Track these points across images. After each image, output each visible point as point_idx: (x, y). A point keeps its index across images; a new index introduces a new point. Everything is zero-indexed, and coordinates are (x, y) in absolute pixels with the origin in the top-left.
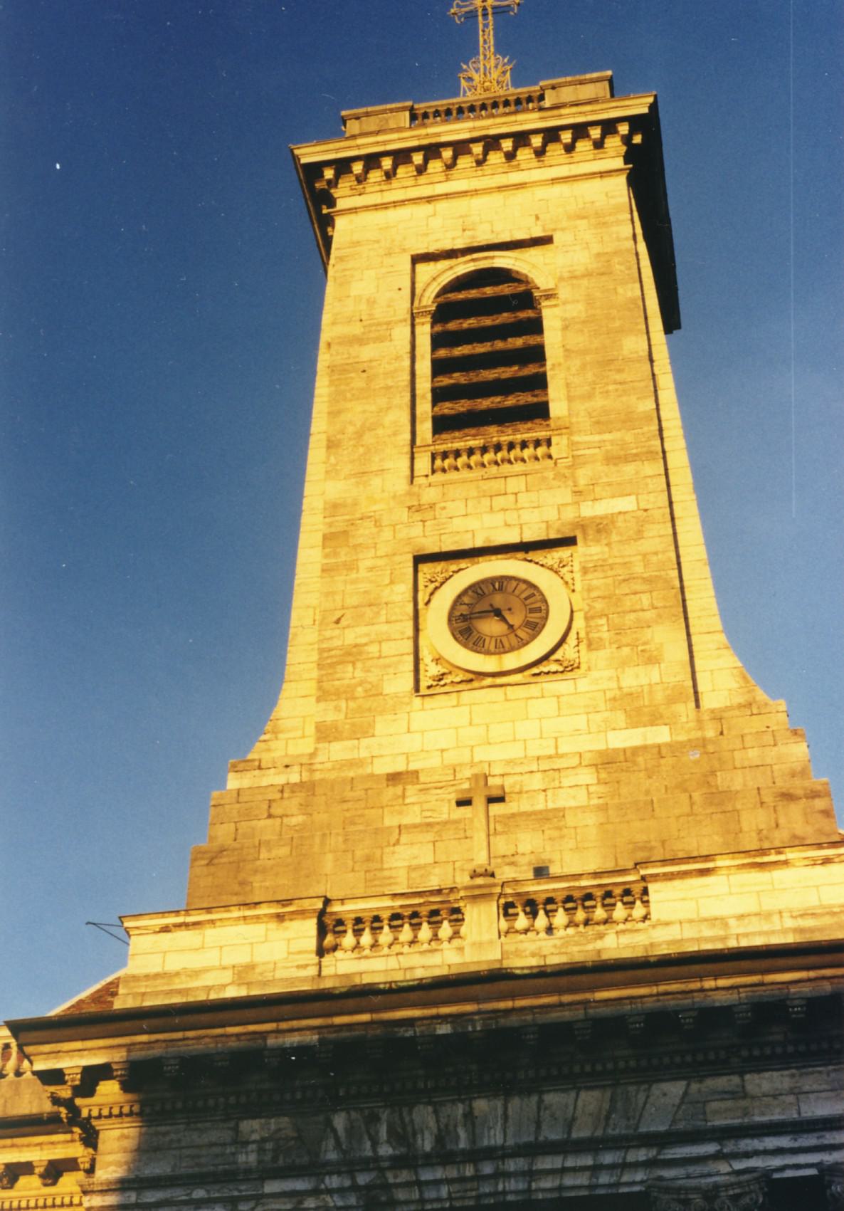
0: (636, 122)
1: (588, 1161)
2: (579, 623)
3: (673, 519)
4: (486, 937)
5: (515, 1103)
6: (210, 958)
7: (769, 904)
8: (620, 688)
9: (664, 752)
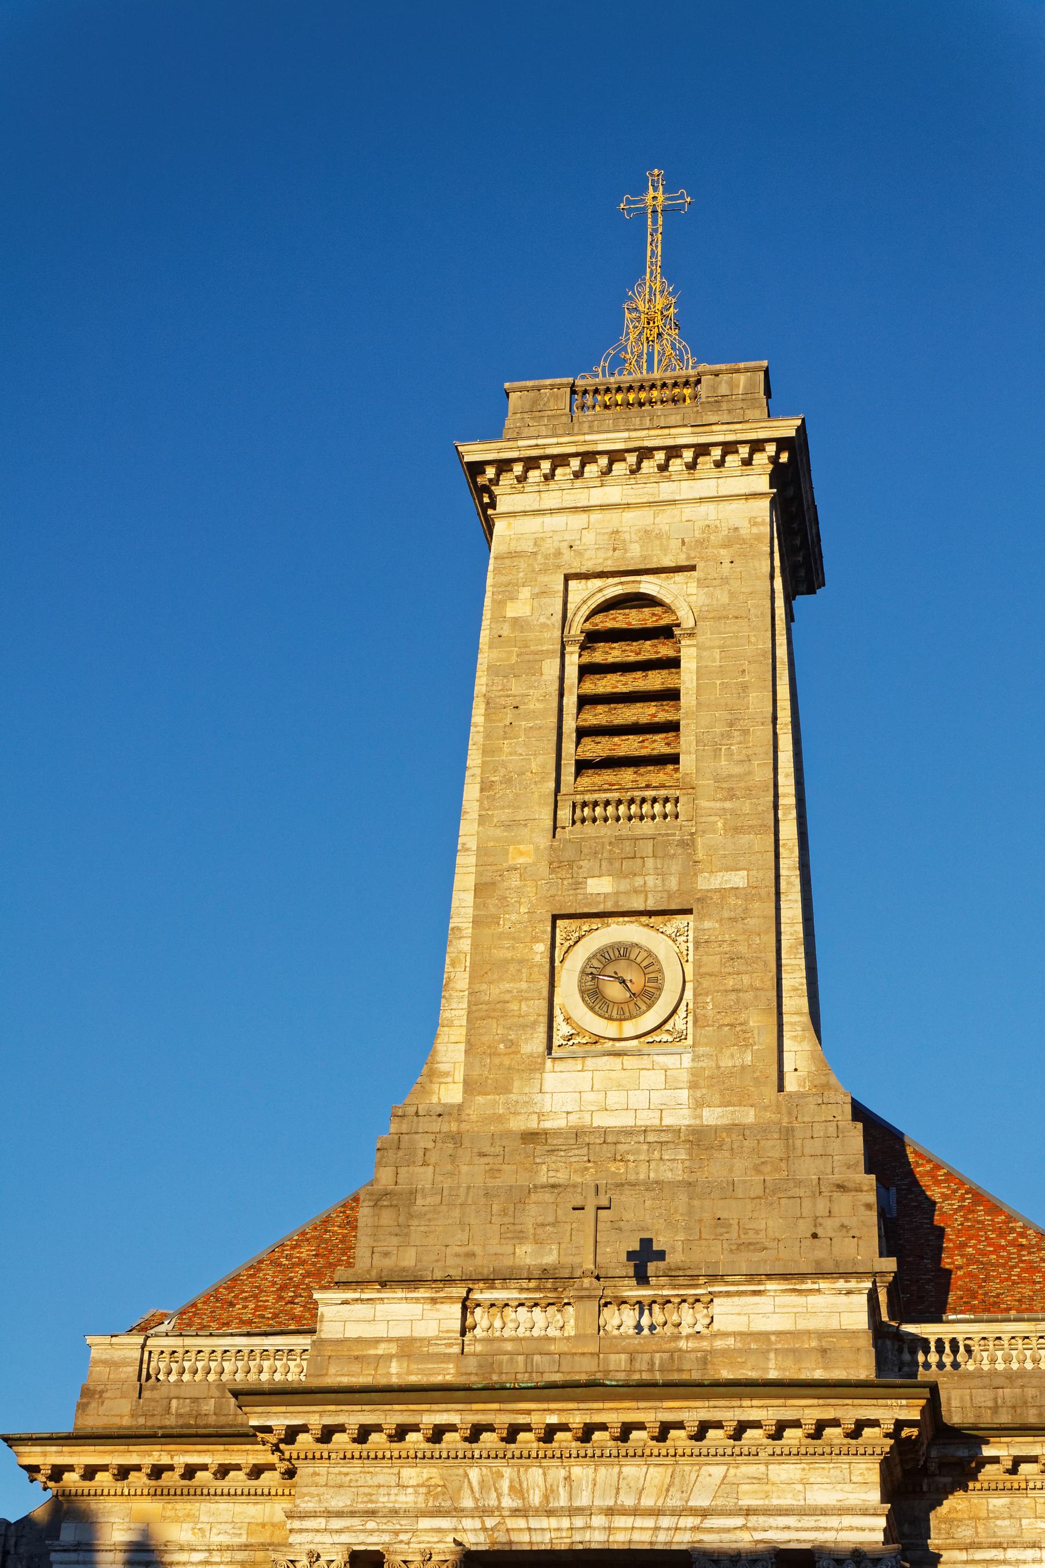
0: (782, 444)
1: (649, 1522)
2: (689, 995)
3: (778, 893)
4: (589, 1331)
5: (602, 1470)
6: (378, 1331)
7: (803, 1325)
8: (718, 1067)
9: (747, 1132)
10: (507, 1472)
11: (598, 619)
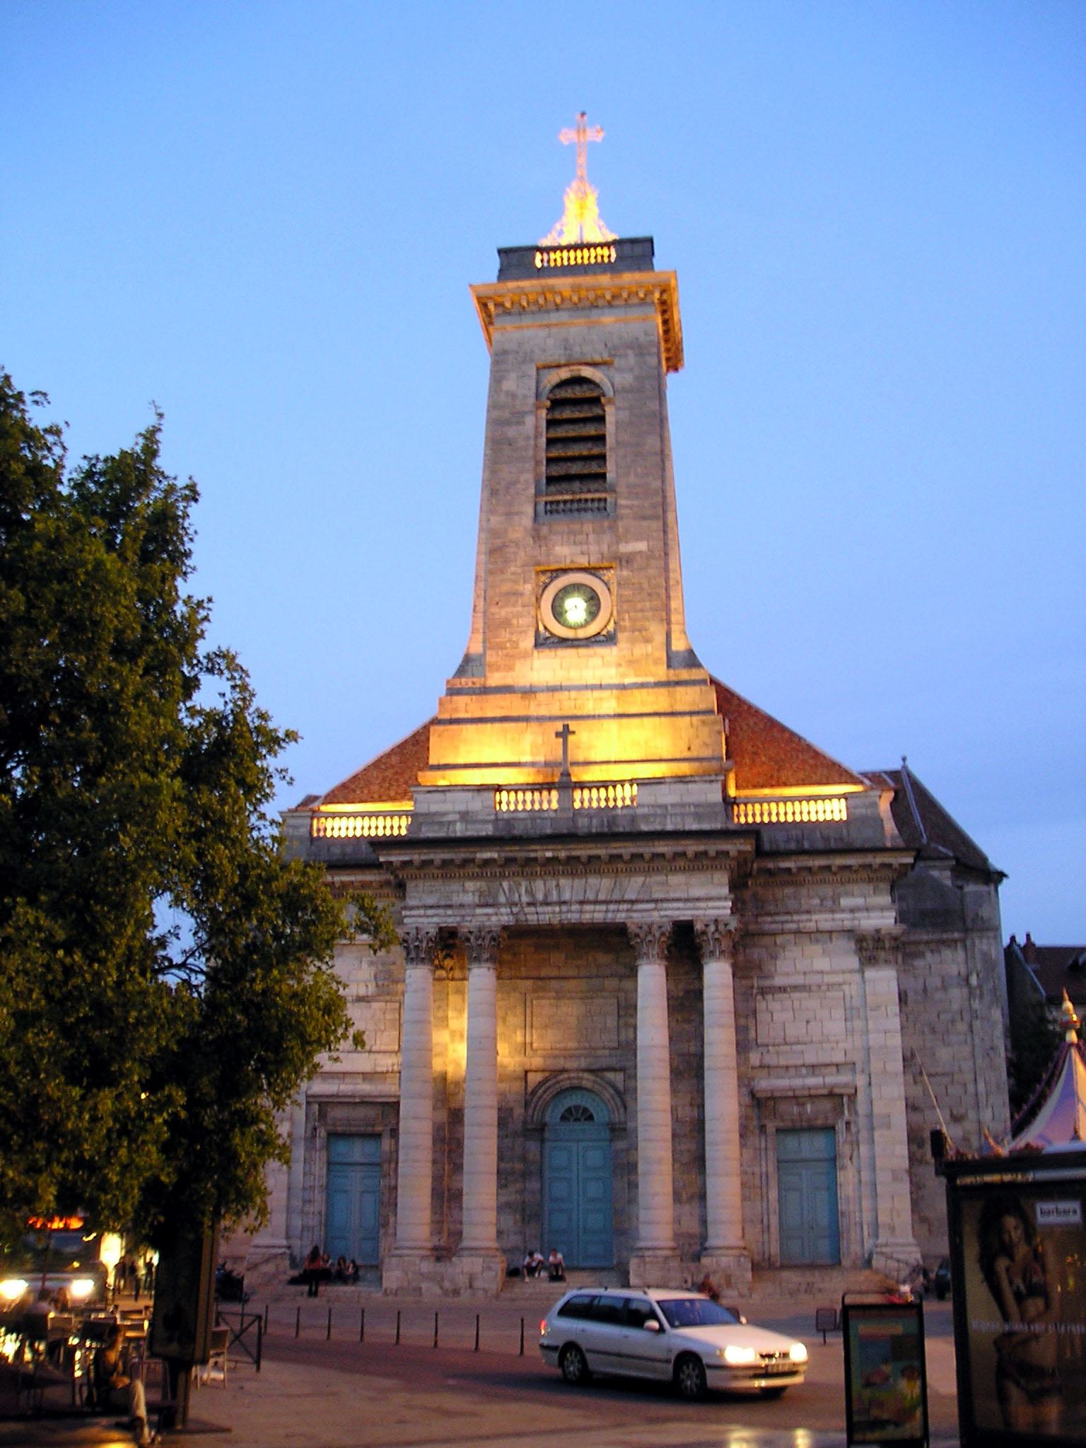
1: (603, 907)
5: (577, 882)
7: (687, 799)
10: (524, 884)
11: (557, 391)
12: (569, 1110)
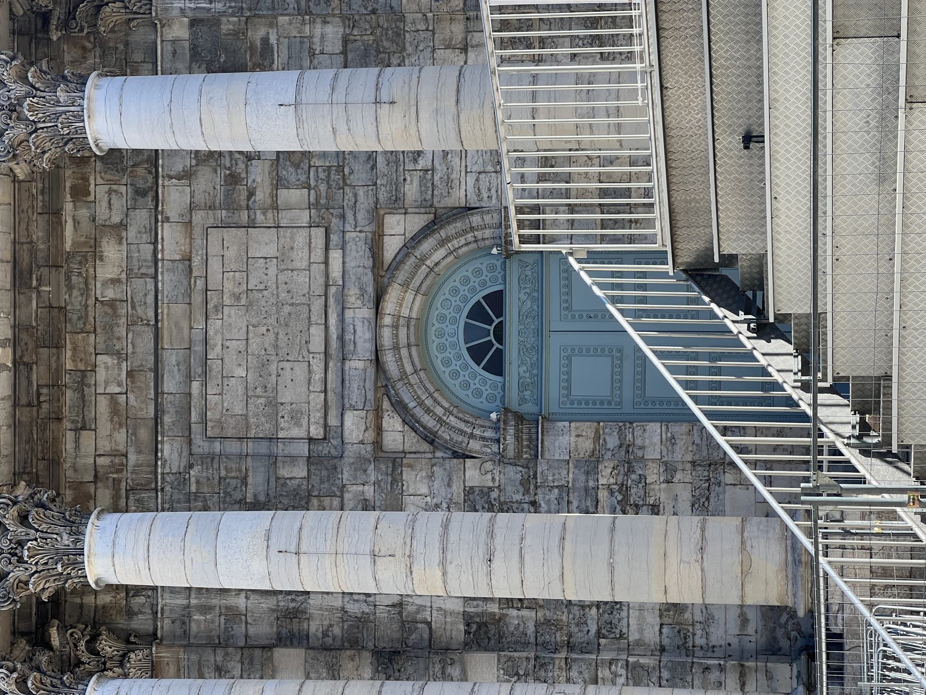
12: (477, 353)
